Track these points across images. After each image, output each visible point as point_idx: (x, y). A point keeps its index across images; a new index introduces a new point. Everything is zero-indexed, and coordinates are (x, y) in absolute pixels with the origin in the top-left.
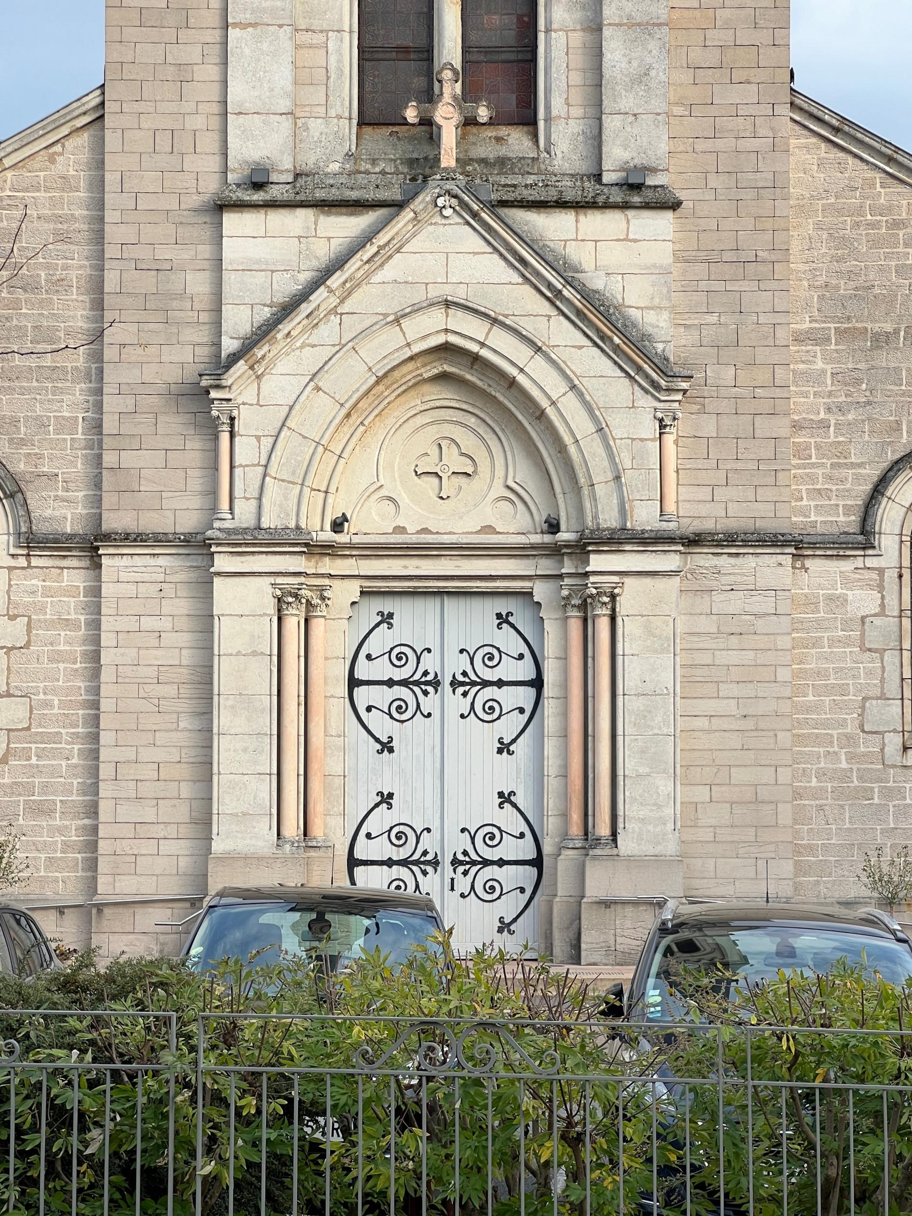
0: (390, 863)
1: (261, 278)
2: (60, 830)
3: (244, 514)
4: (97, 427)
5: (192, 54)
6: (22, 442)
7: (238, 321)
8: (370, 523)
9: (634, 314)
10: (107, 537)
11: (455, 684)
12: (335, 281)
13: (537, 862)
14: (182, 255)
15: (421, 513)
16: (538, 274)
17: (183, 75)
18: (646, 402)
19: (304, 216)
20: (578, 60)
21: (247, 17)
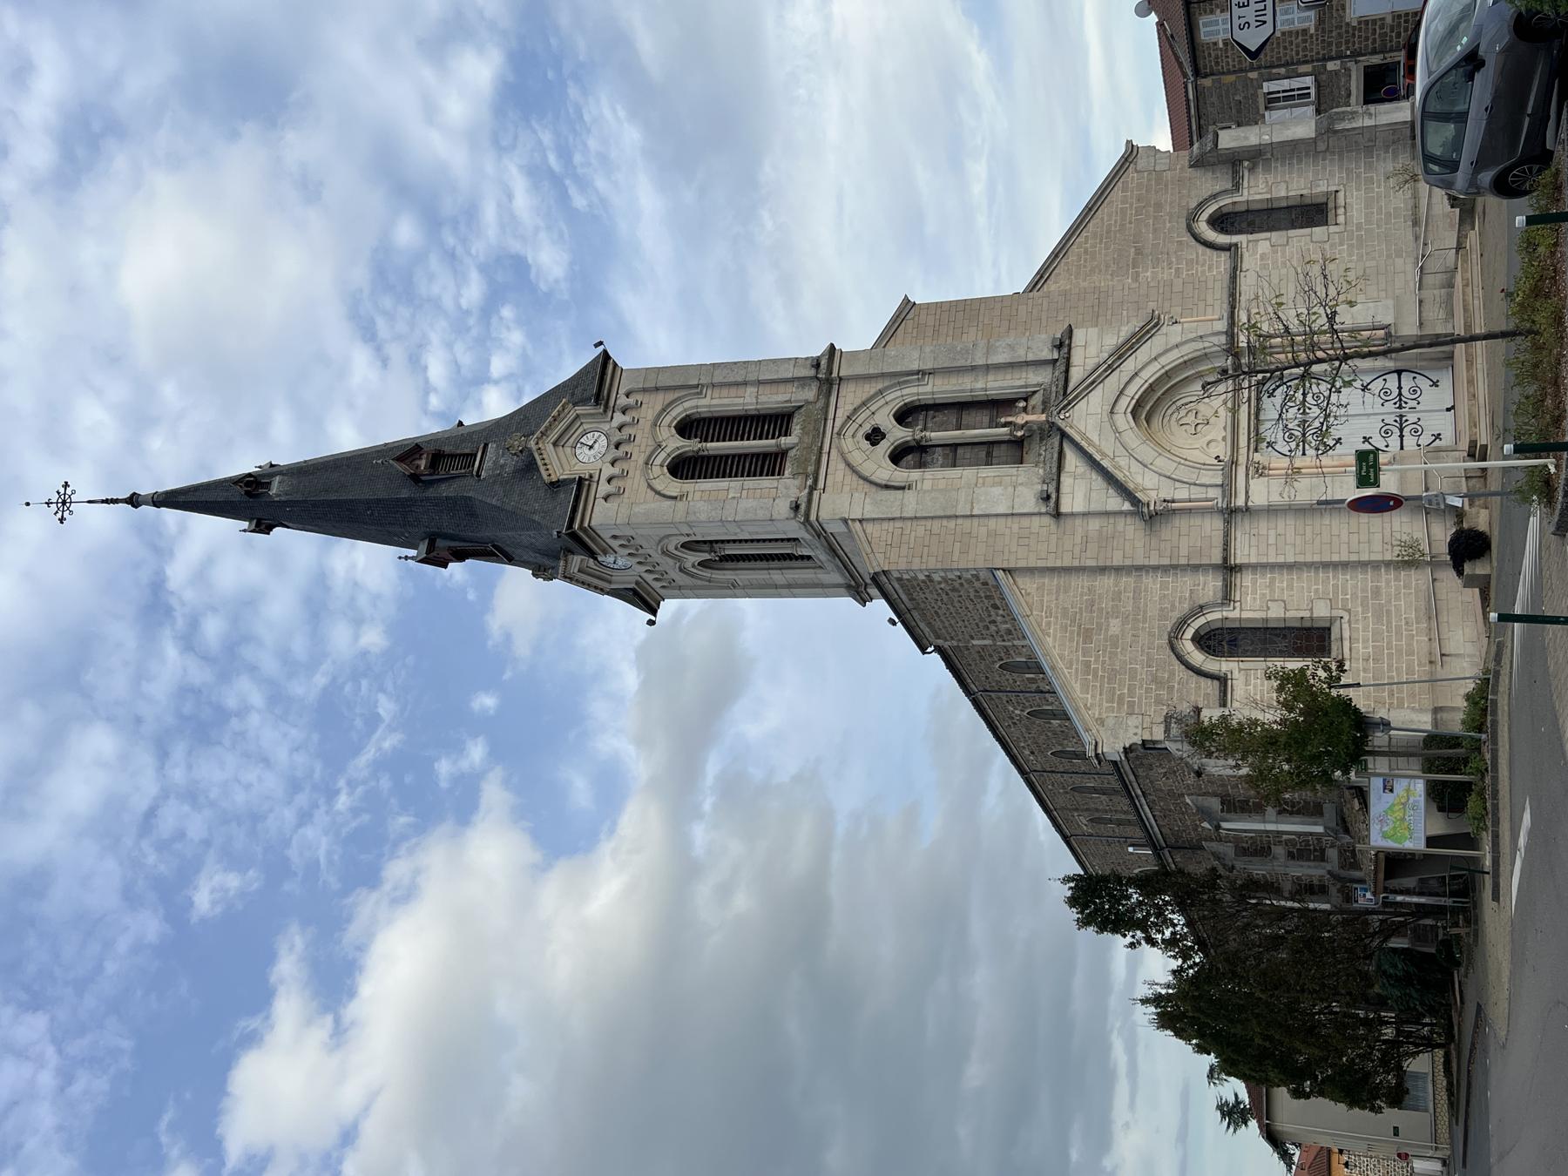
0: (1401, 436)
1: (1094, 494)
2: (1388, 582)
3: (1214, 493)
4: (1165, 569)
5: (983, 530)
6: (1173, 606)
7: (1116, 502)
8: (1222, 450)
9: (1121, 340)
10: (1225, 559)
11: (1304, 413)
12: (1098, 457)
13: (1399, 372)
14: (1079, 532)
15: (1217, 431)
17: (993, 534)
18: (1164, 329)
19: (1066, 481)
20: (1000, 376)
21: (968, 506)
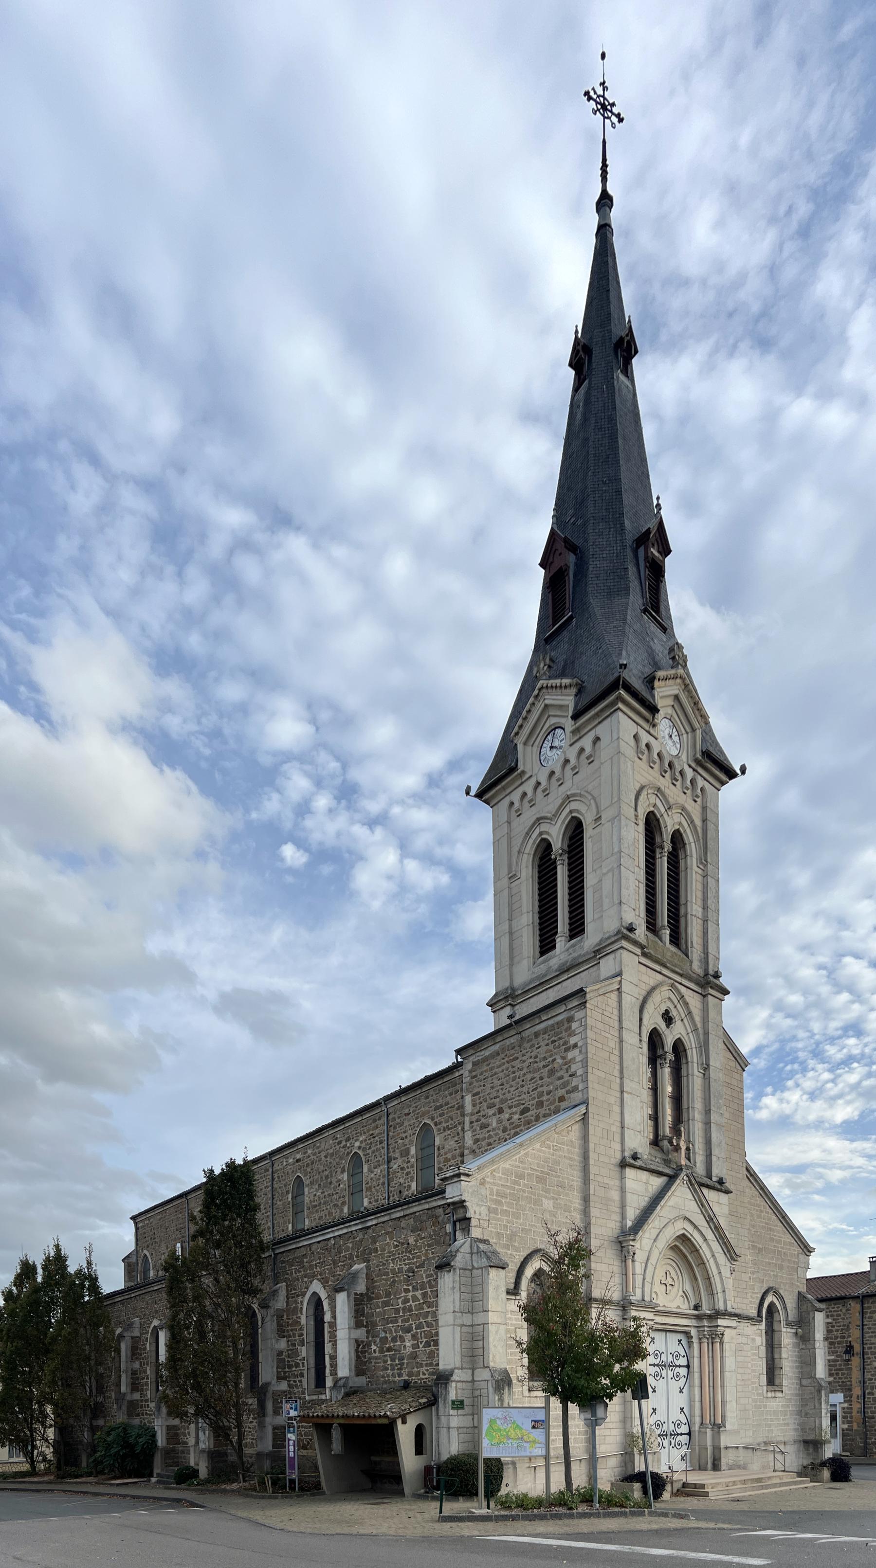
14: (611, 1183)
16: (706, 1210)
18: (729, 1264)
19: (644, 1175)
